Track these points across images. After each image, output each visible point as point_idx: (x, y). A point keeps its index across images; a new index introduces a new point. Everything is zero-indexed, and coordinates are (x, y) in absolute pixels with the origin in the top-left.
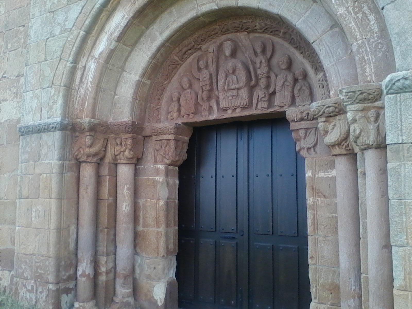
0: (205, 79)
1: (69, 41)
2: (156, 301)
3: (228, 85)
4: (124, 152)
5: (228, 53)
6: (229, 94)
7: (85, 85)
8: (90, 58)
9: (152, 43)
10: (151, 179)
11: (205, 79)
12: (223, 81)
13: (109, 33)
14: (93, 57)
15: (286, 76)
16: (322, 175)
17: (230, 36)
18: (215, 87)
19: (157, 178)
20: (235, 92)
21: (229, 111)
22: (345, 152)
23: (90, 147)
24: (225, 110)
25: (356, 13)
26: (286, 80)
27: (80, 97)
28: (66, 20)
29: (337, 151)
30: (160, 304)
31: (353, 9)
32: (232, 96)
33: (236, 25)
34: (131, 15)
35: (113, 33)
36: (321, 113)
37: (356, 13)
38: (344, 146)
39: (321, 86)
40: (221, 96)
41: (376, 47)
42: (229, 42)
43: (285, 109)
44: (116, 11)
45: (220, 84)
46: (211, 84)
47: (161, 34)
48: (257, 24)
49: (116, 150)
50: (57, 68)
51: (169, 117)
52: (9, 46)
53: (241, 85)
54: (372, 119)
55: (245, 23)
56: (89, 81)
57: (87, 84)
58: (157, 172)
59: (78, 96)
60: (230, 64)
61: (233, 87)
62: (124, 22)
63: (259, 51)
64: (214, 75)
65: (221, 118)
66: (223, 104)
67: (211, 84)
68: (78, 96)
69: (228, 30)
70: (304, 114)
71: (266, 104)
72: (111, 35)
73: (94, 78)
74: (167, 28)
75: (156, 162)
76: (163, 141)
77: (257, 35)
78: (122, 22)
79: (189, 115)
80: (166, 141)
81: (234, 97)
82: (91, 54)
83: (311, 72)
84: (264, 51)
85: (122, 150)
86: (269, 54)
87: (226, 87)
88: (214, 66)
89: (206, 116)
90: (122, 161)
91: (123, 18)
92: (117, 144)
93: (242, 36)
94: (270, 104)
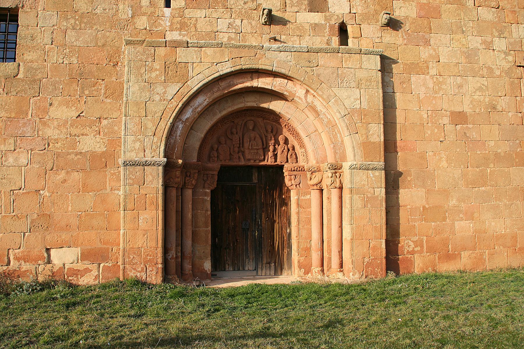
0: (237, 140)
1: (169, 108)
2: (206, 271)
3: (251, 146)
4: (192, 181)
5: (251, 128)
6: (252, 151)
7: (174, 137)
8: (178, 120)
9: (214, 116)
10: (201, 198)
11: (237, 140)
12: (249, 143)
13: (194, 107)
14: (181, 120)
15: (284, 147)
16: (303, 198)
17: (253, 118)
18: (241, 146)
19: (206, 198)
20: (256, 151)
21: (252, 161)
22: (319, 188)
23: (178, 178)
24: (249, 160)
25: (333, 132)
26: (284, 149)
27: (170, 144)
28: (165, 93)
29: (315, 187)
30: (209, 273)
31: (332, 130)
32: (254, 153)
33: (259, 114)
34: (211, 100)
35: (197, 108)
36: (310, 170)
37: (333, 132)
38: (319, 186)
39: (303, 155)
40: (247, 152)
41: (340, 147)
42: (252, 121)
43: (283, 164)
44: (200, 94)
45: (246, 145)
46: (240, 144)
47: (220, 112)
48: (272, 117)
49: (186, 180)
50: (158, 124)
51: (211, 160)
52: (87, 92)
53: (260, 147)
54: (338, 177)
55: (265, 115)
56: (178, 135)
57: (176, 136)
58: (206, 194)
59: (168, 144)
60: (252, 135)
61: (255, 148)
62: (206, 103)
63: (270, 130)
64: (241, 138)
65: (247, 164)
66: (248, 156)
67: (240, 144)
68: (168, 144)
69: (253, 115)
70: (296, 168)
71: (273, 160)
72: (196, 108)
73: (182, 133)
74: (224, 109)
75: (204, 188)
76: (209, 175)
77: (269, 121)
78: (204, 103)
79: (225, 160)
80: (211, 175)
81: (255, 154)
82: (178, 118)
83: (297, 147)
84: (272, 132)
85: (191, 180)
86: (274, 133)
87: (250, 147)
88: (241, 133)
89: (237, 162)
90: (189, 187)
91: (205, 101)
92: (187, 176)
93: (260, 120)
94: (276, 161)
